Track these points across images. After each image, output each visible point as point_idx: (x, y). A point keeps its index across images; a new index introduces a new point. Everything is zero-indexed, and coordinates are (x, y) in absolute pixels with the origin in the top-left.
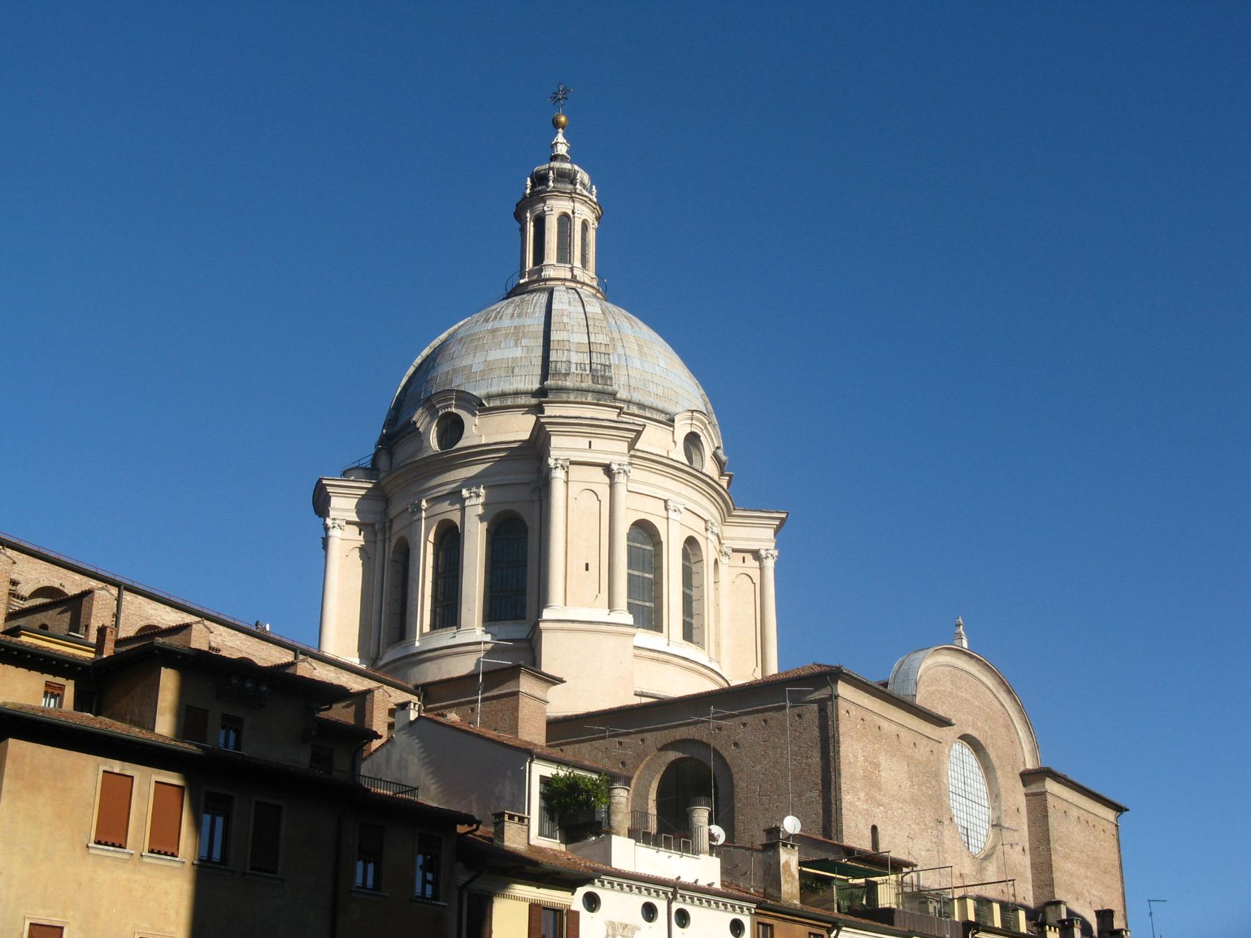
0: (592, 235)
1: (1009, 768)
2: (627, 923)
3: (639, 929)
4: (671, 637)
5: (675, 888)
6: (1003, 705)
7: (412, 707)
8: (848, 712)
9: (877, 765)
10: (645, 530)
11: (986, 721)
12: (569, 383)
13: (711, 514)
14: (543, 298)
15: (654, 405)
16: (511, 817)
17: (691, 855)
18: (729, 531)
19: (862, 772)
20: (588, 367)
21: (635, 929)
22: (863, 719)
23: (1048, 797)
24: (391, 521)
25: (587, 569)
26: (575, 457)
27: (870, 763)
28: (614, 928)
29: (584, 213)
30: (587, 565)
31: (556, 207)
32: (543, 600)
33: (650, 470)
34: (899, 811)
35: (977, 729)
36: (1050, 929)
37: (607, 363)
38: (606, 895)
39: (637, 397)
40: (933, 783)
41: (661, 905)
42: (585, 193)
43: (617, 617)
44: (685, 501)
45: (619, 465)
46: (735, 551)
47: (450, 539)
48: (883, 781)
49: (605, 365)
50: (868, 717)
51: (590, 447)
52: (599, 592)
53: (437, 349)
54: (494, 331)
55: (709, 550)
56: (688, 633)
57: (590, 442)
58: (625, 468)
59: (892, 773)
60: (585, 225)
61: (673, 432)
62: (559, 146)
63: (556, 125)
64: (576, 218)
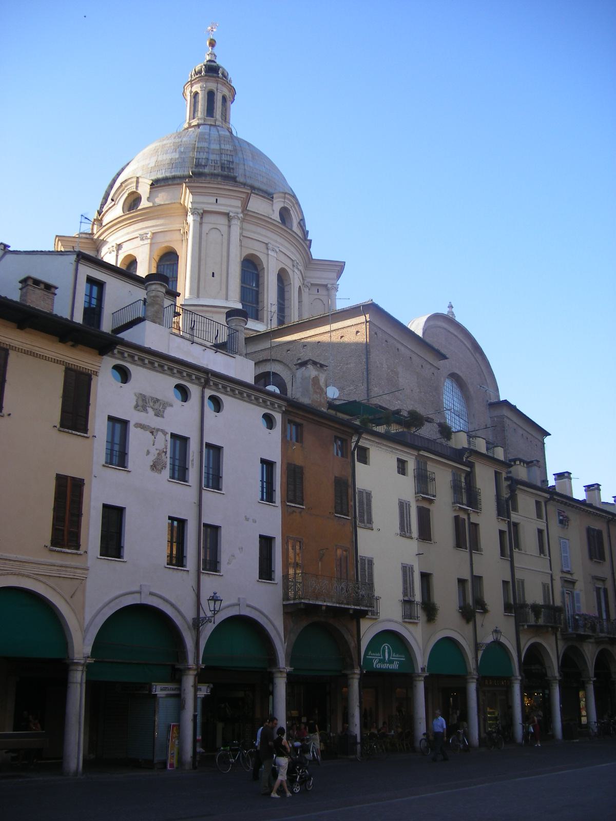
3: (171, 406)
5: (207, 377)
12: (206, 170)
19: (386, 375)
21: (166, 405)
22: (386, 341)
25: (213, 276)
30: (213, 273)
33: (257, 225)
37: (231, 160)
38: (137, 372)
41: (194, 390)
44: (280, 246)
46: (312, 284)
49: (229, 162)
51: (217, 202)
52: (221, 290)
57: (217, 200)
64: (218, 93)
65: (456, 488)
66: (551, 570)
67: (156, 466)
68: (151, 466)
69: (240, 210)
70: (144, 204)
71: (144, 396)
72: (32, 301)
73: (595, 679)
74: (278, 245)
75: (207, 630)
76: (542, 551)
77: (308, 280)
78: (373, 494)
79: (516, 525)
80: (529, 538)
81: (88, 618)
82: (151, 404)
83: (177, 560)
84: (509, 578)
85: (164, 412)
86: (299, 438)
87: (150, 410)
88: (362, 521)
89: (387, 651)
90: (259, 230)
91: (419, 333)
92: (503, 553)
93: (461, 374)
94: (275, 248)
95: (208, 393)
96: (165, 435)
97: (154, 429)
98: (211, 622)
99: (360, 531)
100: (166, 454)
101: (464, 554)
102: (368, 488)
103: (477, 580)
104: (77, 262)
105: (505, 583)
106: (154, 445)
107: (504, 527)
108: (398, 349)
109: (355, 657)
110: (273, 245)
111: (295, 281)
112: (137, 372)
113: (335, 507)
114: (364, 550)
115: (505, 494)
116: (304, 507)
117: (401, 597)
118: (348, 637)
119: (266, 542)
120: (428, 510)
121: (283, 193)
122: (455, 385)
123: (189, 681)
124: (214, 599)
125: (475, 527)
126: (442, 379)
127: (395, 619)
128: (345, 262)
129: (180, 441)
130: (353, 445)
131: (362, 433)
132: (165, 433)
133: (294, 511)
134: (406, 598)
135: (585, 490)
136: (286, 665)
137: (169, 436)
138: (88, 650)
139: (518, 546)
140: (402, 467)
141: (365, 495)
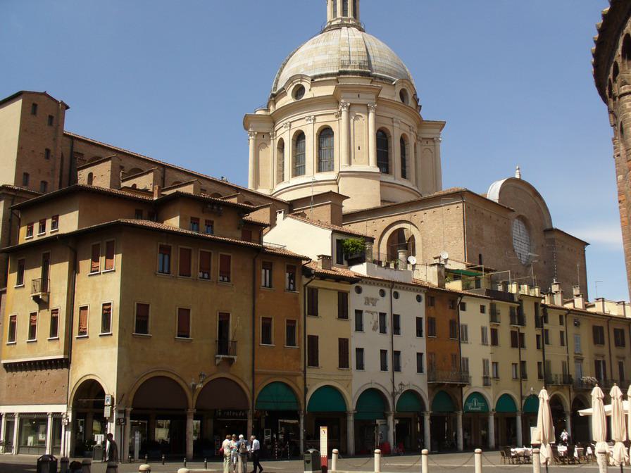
3: (378, 300)
4: (395, 177)
9: (482, 229)
28: (368, 300)
38: (365, 288)
41: (387, 291)
46: (423, 138)
47: (299, 137)
56: (404, 175)
65: (512, 315)
67: (373, 329)
70: (307, 95)
71: (367, 298)
75: (397, 397)
76: (562, 344)
79: (547, 331)
80: (554, 337)
81: (353, 395)
83: (384, 368)
84: (541, 360)
86: (432, 304)
88: (463, 340)
90: (387, 109)
91: (497, 201)
92: (538, 347)
95: (393, 290)
99: (461, 345)
101: (516, 350)
103: (523, 363)
104: (332, 234)
105: (539, 364)
109: (460, 404)
111: (412, 140)
112: (365, 288)
114: (464, 354)
115: (541, 314)
119: (420, 355)
120: (497, 330)
123: (391, 419)
124: (401, 384)
125: (522, 335)
129: (382, 315)
138: (354, 408)
139: (547, 343)
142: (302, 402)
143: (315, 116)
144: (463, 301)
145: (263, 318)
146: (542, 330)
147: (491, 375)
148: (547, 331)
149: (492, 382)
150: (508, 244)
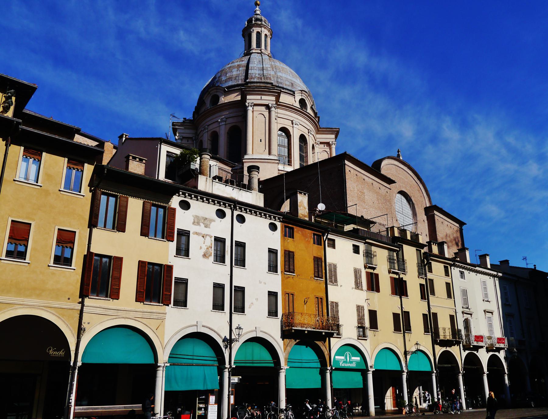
0: (269, 40)
1: (420, 205)
2: (207, 217)
3: (214, 221)
5: (234, 204)
6: (417, 183)
7: (124, 136)
8: (350, 171)
10: (284, 130)
11: (410, 187)
13: (310, 127)
14: (249, 56)
15: (287, 88)
16: (134, 158)
17: (246, 190)
18: (318, 136)
20: (262, 75)
21: (212, 221)
22: (356, 175)
23: (435, 216)
24: (198, 136)
25: (261, 141)
26: (255, 102)
27: (360, 192)
29: (265, 32)
30: (261, 140)
31: (256, 30)
32: (245, 153)
33: (286, 110)
34: (373, 212)
35: (407, 190)
36: (433, 244)
39: (280, 85)
40: (388, 203)
41: (228, 211)
42: (265, 24)
43: (271, 157)
44: (299, 121)
45: (272, 104)
48: (366, 200)
50: (358, 174)
52: (265, 149)
53: (220, 88)
54: (230, 67)
55: (310, 141)
57: (261, 97)
58: (274, 105)
59: (369, 197)
60: (266, 35)
61: (295, 98)
62: (257, 11)
63: (256, 4)
65: (391, 260)
66: (455, 307)
67: (205, 256)
68: (203, 255)
69: (274, 103)
71: (199, 217)
72: (132, 168)
73: (488, 373)
74: (299, 121)
77: (318, 140)
78: (337, 266)
82: (203, 221)
83: (218, 306)
85: (210, 225)
86: (292, 236)
87: (202, 224)
89: (348, 356)
93: (406, 191)
94: (297, 123)
95: (236, 213)
96: (211, 238)
97: (204, 234)
98: (237, 341)
99: (330, 287)
100: (211, 248)
101: (397, 298)
102: (335, 262)
103: (406, 315)
105: (425, 316)
106: (204, 243)
107: (423, 282)
108: (364, 179)
110: (296, 121)
113: (314, 274)
116: (295, 274)
117: (356, 325)
118: (323, 348)
119: (272, 295)
121: (300, 90)
122: (403, 197)
126: (394, 195)
127: (353, 337)
128: (339, 129)
129: (220, 241)
130: (325, 237)
131: (329, 231)
132: (211, 237)
133: (289, 277)
134: (360, 325)
135: (479, 258)
136: (285, 365)
137: (213, 239)
138: (166, 358)
139: (433, 293)
140: (356, 250)
141: (332, 266)
142: (73, 348)
143: (226, 118)
144: (330, 236)
145: (12, 221)
146: (426, 279)
147: (367, 324)
148: (431, 281)
149: (369, 333)
150: (389, 212)
